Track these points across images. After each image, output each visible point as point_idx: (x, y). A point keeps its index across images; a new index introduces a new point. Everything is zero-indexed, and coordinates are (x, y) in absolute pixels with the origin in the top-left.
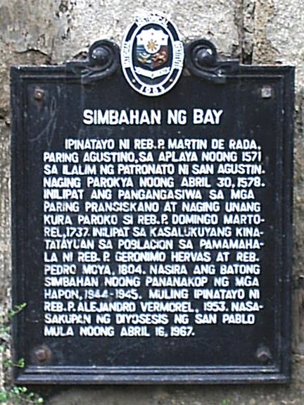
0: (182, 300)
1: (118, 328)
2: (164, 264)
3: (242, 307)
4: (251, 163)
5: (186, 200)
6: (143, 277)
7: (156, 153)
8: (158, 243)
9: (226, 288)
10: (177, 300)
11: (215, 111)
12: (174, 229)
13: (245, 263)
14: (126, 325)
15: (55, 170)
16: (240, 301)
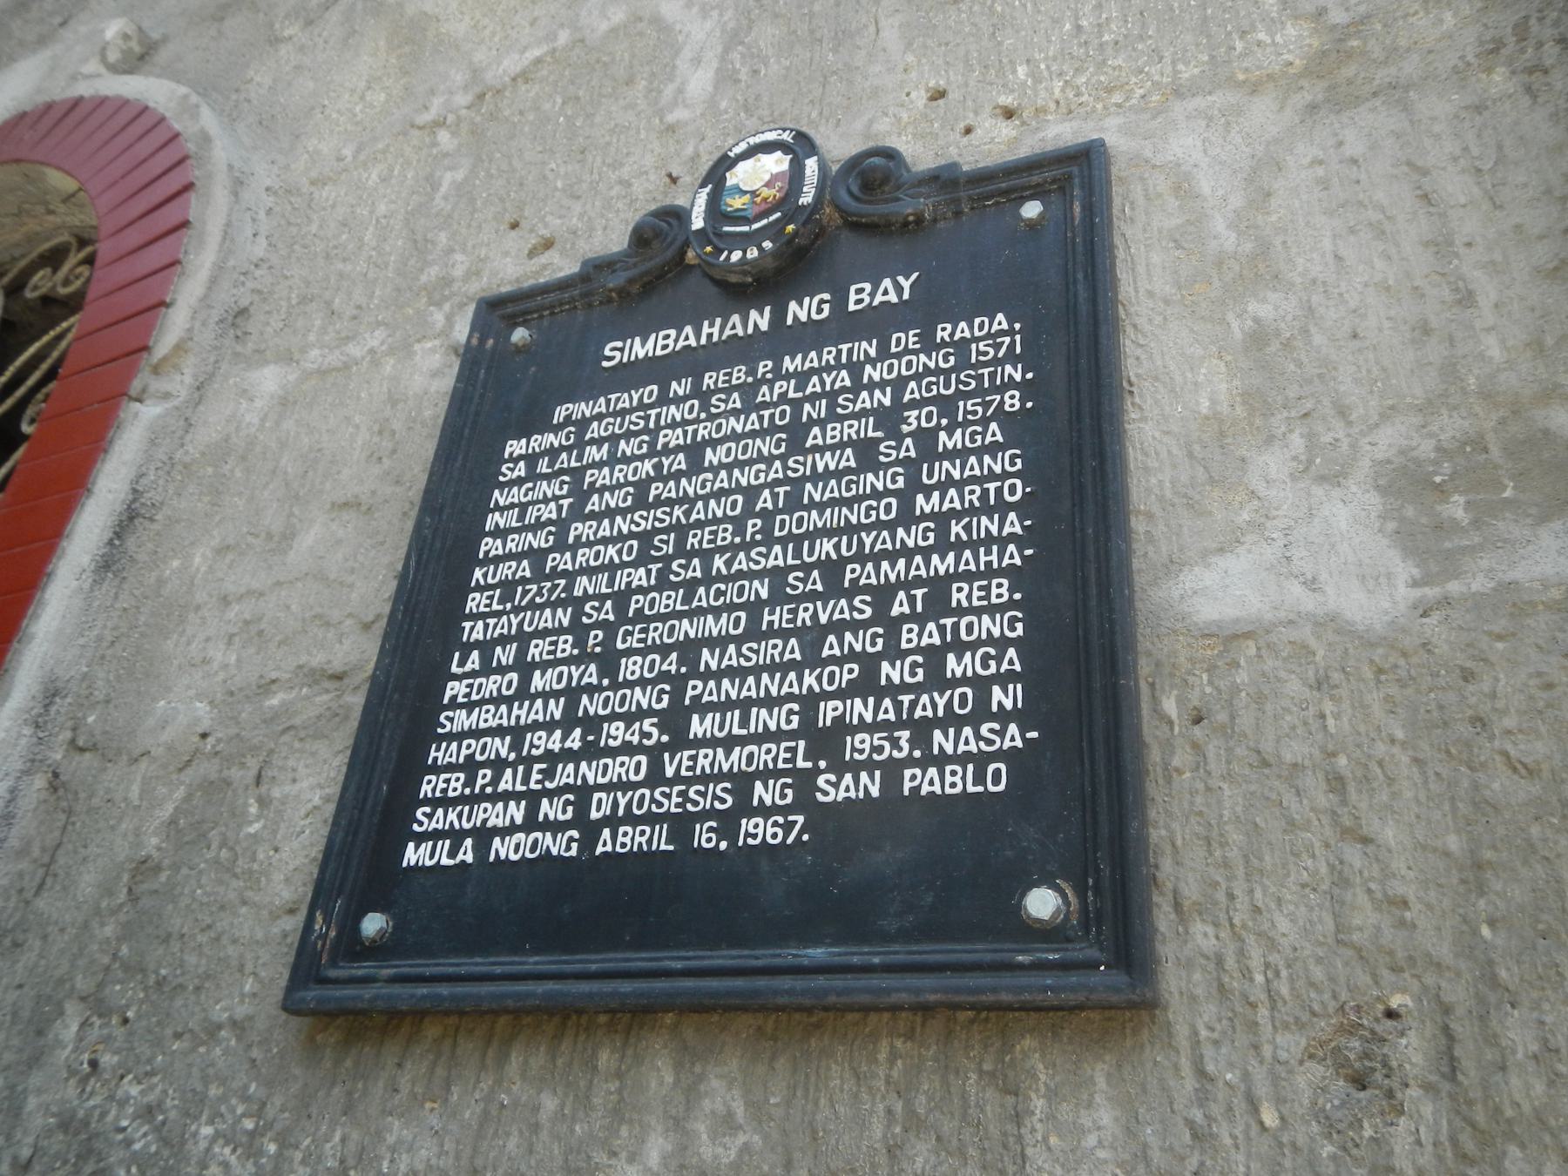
1: (590, 830)
2: (739, 641)
4: (996, 362)
5: (815, 477)
6: (678, 683)
7: (749, 391)
9: (917, 689)
10: (766, 736)
11: (901, 279)
12: (777, 549)
13: (978, 612)
15: (521, 470)
16: (959, 722)
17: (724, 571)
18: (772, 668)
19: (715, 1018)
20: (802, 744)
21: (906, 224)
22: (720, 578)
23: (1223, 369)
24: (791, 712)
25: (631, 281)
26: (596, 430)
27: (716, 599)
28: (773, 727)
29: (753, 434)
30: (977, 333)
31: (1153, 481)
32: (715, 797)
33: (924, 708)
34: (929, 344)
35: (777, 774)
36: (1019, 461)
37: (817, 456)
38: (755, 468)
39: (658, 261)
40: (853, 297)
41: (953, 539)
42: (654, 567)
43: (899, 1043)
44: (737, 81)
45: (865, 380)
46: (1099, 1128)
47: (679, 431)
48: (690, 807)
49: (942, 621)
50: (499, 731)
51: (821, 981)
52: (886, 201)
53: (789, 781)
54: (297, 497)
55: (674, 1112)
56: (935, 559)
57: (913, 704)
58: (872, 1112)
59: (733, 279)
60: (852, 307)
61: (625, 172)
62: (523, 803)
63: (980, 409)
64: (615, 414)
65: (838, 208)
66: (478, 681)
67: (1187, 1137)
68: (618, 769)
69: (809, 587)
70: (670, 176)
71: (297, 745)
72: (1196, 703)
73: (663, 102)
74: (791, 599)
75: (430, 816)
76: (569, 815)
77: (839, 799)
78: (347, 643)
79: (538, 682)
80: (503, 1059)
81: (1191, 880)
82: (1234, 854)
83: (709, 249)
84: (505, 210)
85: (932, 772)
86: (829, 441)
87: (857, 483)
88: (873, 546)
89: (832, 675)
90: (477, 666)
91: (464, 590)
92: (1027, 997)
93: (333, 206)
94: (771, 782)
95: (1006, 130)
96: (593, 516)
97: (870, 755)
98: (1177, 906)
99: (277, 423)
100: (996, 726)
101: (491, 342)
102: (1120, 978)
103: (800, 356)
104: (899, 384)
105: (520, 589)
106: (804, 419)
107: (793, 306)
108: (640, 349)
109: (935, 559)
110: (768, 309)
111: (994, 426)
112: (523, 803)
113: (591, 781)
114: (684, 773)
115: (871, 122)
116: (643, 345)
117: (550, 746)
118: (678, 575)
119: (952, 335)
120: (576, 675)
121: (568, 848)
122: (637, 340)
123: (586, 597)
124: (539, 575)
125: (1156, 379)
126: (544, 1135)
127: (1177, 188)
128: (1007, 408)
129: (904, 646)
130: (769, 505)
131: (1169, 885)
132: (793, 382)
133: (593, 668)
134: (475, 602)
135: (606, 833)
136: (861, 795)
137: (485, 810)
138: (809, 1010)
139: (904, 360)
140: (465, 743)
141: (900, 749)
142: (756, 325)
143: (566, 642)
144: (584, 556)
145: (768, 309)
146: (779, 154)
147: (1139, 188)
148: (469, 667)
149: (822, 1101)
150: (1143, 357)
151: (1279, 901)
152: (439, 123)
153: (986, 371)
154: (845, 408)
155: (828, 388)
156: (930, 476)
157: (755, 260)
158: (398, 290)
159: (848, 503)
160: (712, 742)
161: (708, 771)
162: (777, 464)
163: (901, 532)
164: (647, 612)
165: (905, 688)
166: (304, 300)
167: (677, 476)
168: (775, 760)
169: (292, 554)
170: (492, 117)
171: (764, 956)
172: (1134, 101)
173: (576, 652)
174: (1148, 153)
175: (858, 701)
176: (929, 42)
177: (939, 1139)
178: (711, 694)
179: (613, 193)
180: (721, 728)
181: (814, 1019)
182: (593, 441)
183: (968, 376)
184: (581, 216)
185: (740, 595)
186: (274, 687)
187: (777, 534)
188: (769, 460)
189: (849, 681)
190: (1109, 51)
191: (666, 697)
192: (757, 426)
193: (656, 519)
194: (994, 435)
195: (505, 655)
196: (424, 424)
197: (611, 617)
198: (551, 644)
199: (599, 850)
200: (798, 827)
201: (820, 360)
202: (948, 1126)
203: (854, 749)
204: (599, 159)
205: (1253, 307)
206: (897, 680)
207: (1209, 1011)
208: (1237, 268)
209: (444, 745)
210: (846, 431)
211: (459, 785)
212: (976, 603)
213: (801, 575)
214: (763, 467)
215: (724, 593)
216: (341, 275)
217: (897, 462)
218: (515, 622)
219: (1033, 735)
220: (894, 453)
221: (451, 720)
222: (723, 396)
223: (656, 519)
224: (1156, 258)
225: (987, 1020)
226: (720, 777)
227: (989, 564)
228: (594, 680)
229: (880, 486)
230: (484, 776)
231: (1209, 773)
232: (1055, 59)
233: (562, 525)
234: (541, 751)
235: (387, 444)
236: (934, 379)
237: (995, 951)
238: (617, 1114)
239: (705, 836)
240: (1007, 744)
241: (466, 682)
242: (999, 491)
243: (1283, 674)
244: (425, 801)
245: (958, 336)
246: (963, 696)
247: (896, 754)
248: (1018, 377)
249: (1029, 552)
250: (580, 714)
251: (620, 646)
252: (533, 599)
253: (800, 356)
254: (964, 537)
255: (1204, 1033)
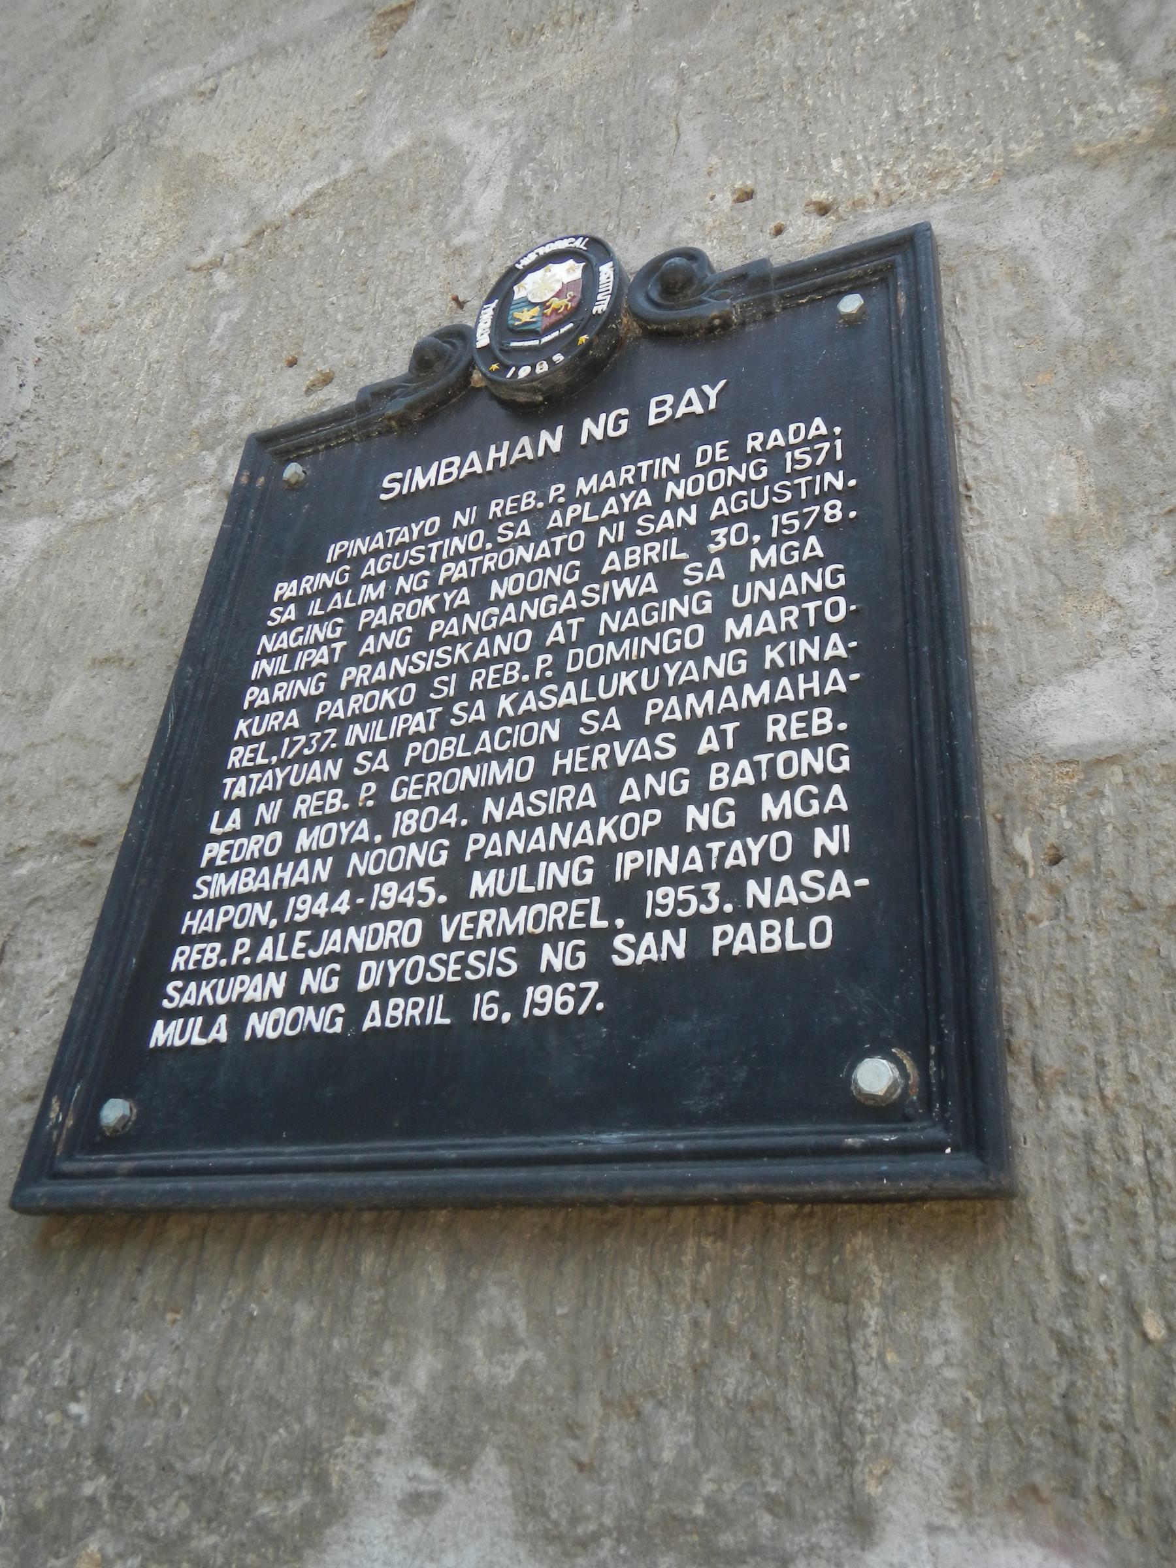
0: (569, 893)
1: (357, 1004)
3: (788, 892)
4: (814, 470)
5: (612, 606)
6: (458, 837)
7: (538, 517)
8: (519, 732)
11: (706, 388)
12: (570, 685)
13: (797, 745)
14: (382, 993)
15: (291, 613)
17: (511, 713)
18: (563, 817)
19: (495, 1215)
20: (596, 901)
21: (711, 329)
22: (506, 720)
23: (1074, 465)
24: (584, 865)
25: (411, 407)
26: (373, 567)
27: (501, 743)
28: (563, 882)
29: (544, 563)
30: (792, 441)
31: (997, 593)
32: (497, 963)
33: (736, 857)
34: (738, 456)
35: (568, 935)
36: (841, 577)
37: (615, 583)
38: (545, 599)
39: (441, 383)
40: (653, 410)
41: (767, 666)
42: (434, 712)
43: (707, 1243)
44: (528, 199)
45: (668, 498)
46: (946, 1343)
47: (463, 564)
48: (469, 975)
49: (756, 758)
50: (259, 896)
51: (615, 1171)
52: (690, 305)
53: (582, 942)
54: (56, 655)
55: (445, 1324)
56: (748, 689)
57: (724, 852)
58: (675, 1325)
59: (522, 398)
60: (652, 421)
61: (409, 300)
62: (284, 974)
63: (796, 523)
64: (394, 549)
65: (636, 316)
66: (239, 841)
67: (1053, 1353)
68: (389, 935)
69: (605, 726)
70: (456, 299)
71: (44, 917)
72: (1053, 840)
73: (449, 226)
74: (585, 740)
75: (181, 991)
76: (334, 986)
77: (639, 962)
78: (102, 806)
79: (304, 841)
80: (254, 1263)
81: (1052, 1046)
82: (1103, 1013)
83: (495, 366)
84: (282, 347)
85: (746, 928)
86: (627, 566)
87: (659, 610)
88: (677, 678)
89: (631, 823)
90: (238, 826)
91: (227, 743)
92: (858, 1186)
93: (104, 354)
94: (561, 945)
95: (821, 228)
96: (369, 659)
97: (674, 911)
98: (1036, 1076)
99: (39, 578)
100: (820, 874)
101: (262, 480)
102: (968, 1162)
103: (595, 477)
104: (706, 501)
105: (287, 740)
106: (600, 543)
107: (588, 424)
108: (420, 479)
109: (748, 689)
110: (560, 429)
111: (812, 540)
112: (284, 974)
113: (359, 949)
114: (463, 937)
115: (673, 228)
116: (424, 475)
117: (315, 911)
118: (459, 718)
119: (764, 444)
120: (345, 832)
121: (332, 1024)
122: (418, 470)
123: (359, 747)
124: (308, 725)
125: (997, 480)
126: (297, 1351)
127: (1014, 274)
128: (827, 519)
129: (713, 786)
130: (561, 639)
131: (1027, 1053)
132: (587, 505)
133: (364, 823)
134: (238, 756)
135: (375, 1006)
136: (664, 956)
137: (242, 983)
138: (602, 1205)
139: (711, 474)
140: (223, 909)
141: (709, 903)
142: (547, 446)
143: (335, 796)
144: (360, 701)
145: (560, 429)
146: (571, 262)
147: (971, 276)
148: (229, 827)
149: (618, 1312)
150: (981, 458)
151: (1159, 1067)
152: (216, 264)
153: (803, 481)
154: (645, 529)
155: (626, 509)
156: (741, 598)
157: (545, 375)
158: (169, 436)
159: (649, 632)
160: (494, 902)
161: (490, 934)
162: (570, 594)
163: (708, 661)
164: (425, 760)
165: (714, 834)
166: (71, 451)
167: (460, 612)
168: (566, 920)
169: (48, 715)
170: (271, 254)
171: (551, 1143)
172: (961, 186)
173: (346, 806)
174: (979, 239)
175: (660, 851)
176: (735, 142)
177: (754, 1356)
178: (494, 848)
179: (396, 322)
180: (506, 886)
181: (608, 1216)
182: (369, 580)
183: (782, 487)
184: (362, 348)
185: (528, 737)
186: (23, 856)
187: (570, 669)
188: (561, 590)
189: (650, 829)
190: (933, 136)
191: (444, 854)
192: (548, 554)
193: (436, 659)
194: (813, 549)
195: (268, 813)
196: (191, 572)
197: (386, 767)
198: (319, 798)
199: (367, 1025)
200: (591, 995)
201: (617, 479)
202: (764, 1341)
203: (655, 905)
204: (382, 289)
205: (1105, 396)
206: (704, 826)
207: (1078, 1200)
208: (1085, 355)
209: (200, 912)
210: (647, 554)
211: (214, 956)
212: (794, 736)
213: (596, 713)
214: (554, 597)
215: (510, 737)
216: (110, 423)
217: (705, 585)
218: (280, 776)
219: (863, 882)
220: (700, 575)
221: (208, 884)
222: (511, 524)
223: (436, 659)
224: (992, 350)
225: (811, 1215)
226: (502, 941)
227: (809, 692)
228: (365, 837)
229: (685, 612)
230: (242, 946)
231: (1071, 920)
232: (872, 148)
233: (334, 670)
234: (305, 916)
235: (153, 596)
236: (744, 493)
237: (820, 1133)
238: (381, 1326)
239: (485, 1007)
240: (833, 894)
241: (225, 843)
242: (819, 611)
243: (1156, 803)
244: (178, 975)
245: (770, 444)
246: (781, 842)
247: (704, 909)
248: (839, 485)
249: (855, 677)
250: (349, 874)
251: (394, 798)
252: (301, 750)
253: (595, 477)
254: (781, 663)
255: (1071, 1227)
